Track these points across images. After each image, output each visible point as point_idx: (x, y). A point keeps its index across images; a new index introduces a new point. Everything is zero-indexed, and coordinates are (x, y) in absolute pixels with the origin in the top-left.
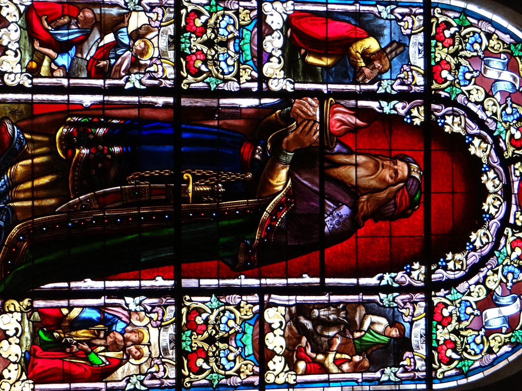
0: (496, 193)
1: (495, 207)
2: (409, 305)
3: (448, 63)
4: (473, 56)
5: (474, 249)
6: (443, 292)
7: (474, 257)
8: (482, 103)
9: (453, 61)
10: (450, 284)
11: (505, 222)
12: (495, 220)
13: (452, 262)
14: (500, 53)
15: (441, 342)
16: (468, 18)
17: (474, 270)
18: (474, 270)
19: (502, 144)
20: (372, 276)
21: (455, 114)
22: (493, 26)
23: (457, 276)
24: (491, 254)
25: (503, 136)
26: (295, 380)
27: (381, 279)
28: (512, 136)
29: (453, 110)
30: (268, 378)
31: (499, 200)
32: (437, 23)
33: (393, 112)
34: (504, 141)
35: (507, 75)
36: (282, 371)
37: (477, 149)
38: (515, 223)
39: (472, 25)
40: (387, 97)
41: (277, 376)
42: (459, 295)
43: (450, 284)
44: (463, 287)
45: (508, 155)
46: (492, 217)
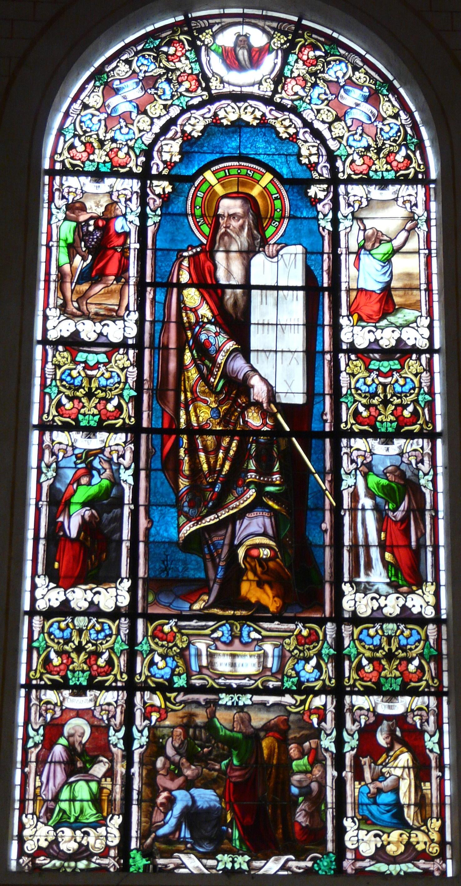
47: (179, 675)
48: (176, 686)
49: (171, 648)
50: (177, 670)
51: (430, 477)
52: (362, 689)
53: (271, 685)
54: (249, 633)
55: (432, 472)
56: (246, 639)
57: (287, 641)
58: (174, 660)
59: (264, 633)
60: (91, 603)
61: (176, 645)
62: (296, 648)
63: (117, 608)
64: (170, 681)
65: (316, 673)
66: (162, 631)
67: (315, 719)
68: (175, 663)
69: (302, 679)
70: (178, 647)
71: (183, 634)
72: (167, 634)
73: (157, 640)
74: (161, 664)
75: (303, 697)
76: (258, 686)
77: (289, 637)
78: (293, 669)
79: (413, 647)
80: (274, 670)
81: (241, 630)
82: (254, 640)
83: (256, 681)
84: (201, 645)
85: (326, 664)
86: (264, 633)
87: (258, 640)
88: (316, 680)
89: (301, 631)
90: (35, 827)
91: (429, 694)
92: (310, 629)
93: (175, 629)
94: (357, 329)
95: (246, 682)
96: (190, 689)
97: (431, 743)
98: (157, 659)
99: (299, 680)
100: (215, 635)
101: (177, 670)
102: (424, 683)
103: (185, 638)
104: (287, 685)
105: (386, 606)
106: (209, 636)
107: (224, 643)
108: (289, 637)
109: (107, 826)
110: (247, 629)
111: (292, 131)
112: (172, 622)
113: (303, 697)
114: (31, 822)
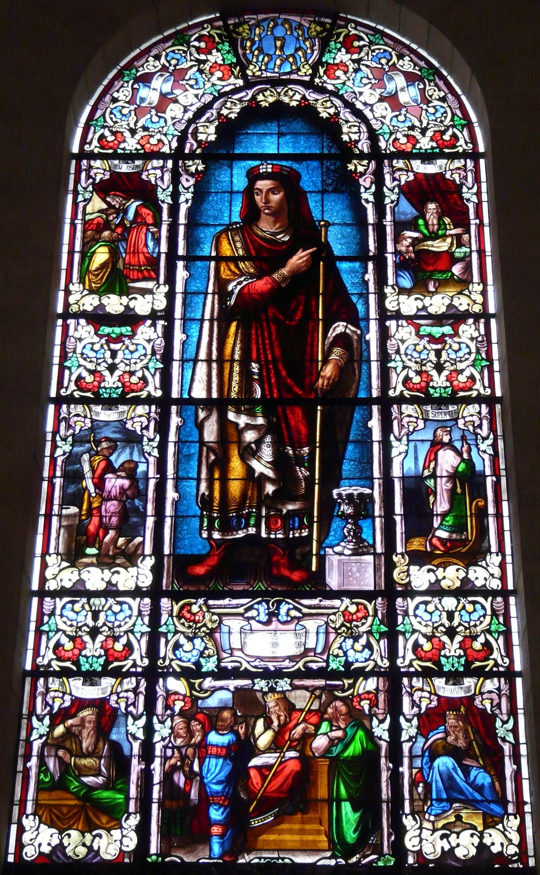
0: (279, 94)
1: (294, 94)
2: (397, 175)
3: (142, 138)
4: (135, 115)
5: (337, 114)
6: (382, 144)
7: (346, 114)
8: (185, 107)
9: (141, 134)
10: (373, 136)
11: (308, 85)
12: (307, 95)
13: (351, 135)
14: (133, 89)
15: (434, 145)
16: (96, 118)
17: (358, 114)
18: (358, 114)
19: (227, 89)
20: (365, 209)
21: (195, 132)
22: (105, 96)
23: (365, 130)
24: (341, 98)
25: (219, 88)
26: (479, 284)
27: (367, 201)
28: (220, 79)
29: (192, 134)
30: (477, 311)
31: (287, 91)
32: (100, 148)
33: (192, 189)
34: (223, 86)
35: (156, 82)
36: (469, 297)
37: (232, 111)
38: (310, 75)
39: (104, 115)
40: (175, 195)
41: (474, 302)
42: (385, 127)
43: (373, 136)
44: (376, 125)
45: (240, 82)
46: (304, 97)
47: (209, 656)
48: (204, 670)
49: (199, 628)
50: (206, 652)
51: (490, 442)
52: (420, 670)
53: (314, 666)
54: (289, 610)
55: (492, 436)
56: (283, 617)
57: (332, 617)
58: (203, 641)
59: (305, 610)
60: (109, 583)
61: (205, 625)
62: (343, 625)
63: (138, 588)
64: (198, 664)
65: (367, 652)
66: (189, 611)
67: (365, 705)
68: (203, 644)
69: (350, 659)
70: (208, 628)
71: (213, 614)
72: (195, 615)
73: (183, 620)
74: (188, 646)
75: (351, 681)
76: (299, 668)
77: (334, 614)
78: (340, 648)
79: (478, 623)
80: (319, 650)
81: (278, 608)
82: (293, 618)
83: (297, 662)
84: (235, 624)
85: (378, 641)
86: (305, 610)
87: (299, 619)
88: (367, 660)
89: (347, 607)
90: (37, 829)
91: (499, 675)
92: (357, 604)
93: (204, 609)
94: (414, 569)
95: (287, 663)
96: (222, 673)
97: (502, 729)
98: (183, 640)
99: (347, 661)
100: (249, 614)
101: (206, 652)
102: (491, 663)
103: (215, 618)
104: (333, 665)
105: (444, 578)
106: (241, 615)
107: (259, 622)
108: (334, 614)
109: (121, 827)
110: (287, 606)
111: (332, 111)
112: (201, 601)
113: (351, 681)
114: (33, 824)
